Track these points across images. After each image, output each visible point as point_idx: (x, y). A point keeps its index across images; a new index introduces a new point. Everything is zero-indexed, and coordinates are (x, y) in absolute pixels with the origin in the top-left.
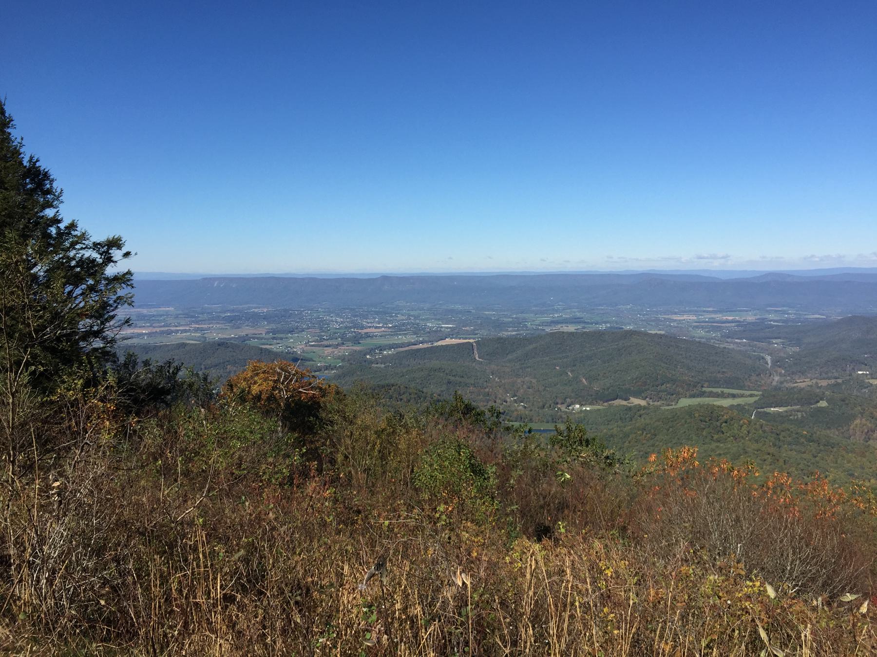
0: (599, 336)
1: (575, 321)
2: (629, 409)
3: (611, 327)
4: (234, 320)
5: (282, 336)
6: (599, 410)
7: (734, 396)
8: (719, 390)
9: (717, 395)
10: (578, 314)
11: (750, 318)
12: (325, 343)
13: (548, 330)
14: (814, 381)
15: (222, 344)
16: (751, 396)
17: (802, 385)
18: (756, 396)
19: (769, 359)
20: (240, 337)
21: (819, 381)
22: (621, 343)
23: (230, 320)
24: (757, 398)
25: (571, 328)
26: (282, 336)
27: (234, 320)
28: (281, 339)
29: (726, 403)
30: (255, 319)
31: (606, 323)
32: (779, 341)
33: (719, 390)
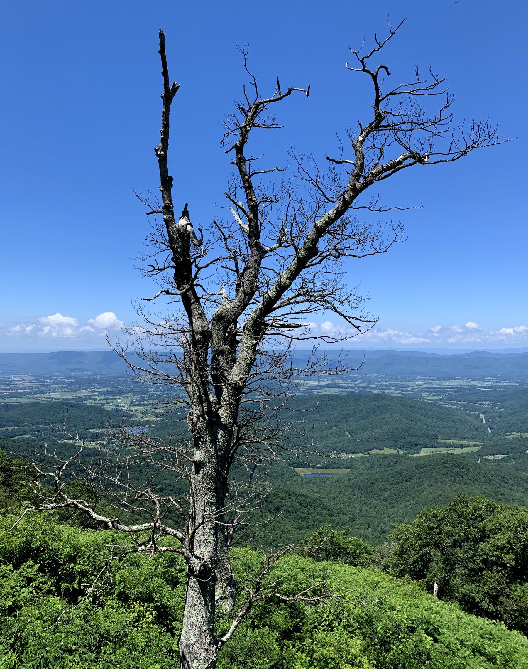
0: (356, 397)
1: (335, 385)
2: (386, 457)
3: (363, 391)
4: (74, 386)
5: (110, 397)
6: (362, 458)
7: (462, 446)
8: (451, 441)
9: (450, 446)
10: (336, 381)
11: (463, 383)
12: (145, 402)
13: (315, 392)
14: (519, 434)
15: (66, 403)
16: (475, 446)
17: (511, 437)
18: (479, 446)
19: (482, 416)
20: (79, 398)
21: (522, 434)
22: (373, 404)
23: (70, 384)
24: (479, 448)
25: (334, 391)
26: (110, 397)
27: (74, 386)
28: (111, 399)
29: (457, 451)
30: (89, 383)
31: (359, 387)
32: (487, 403)
33: (451, 441)
